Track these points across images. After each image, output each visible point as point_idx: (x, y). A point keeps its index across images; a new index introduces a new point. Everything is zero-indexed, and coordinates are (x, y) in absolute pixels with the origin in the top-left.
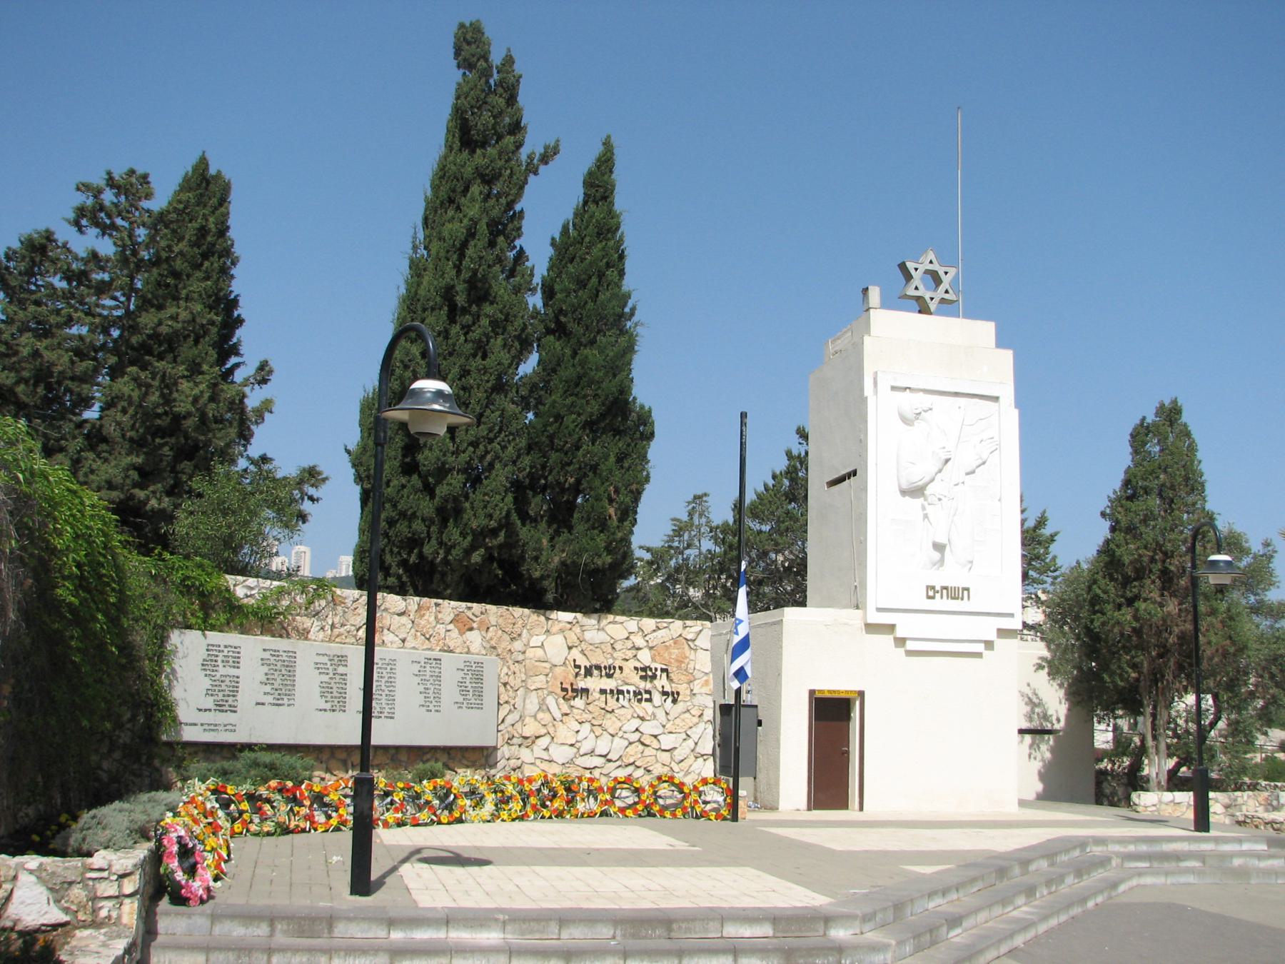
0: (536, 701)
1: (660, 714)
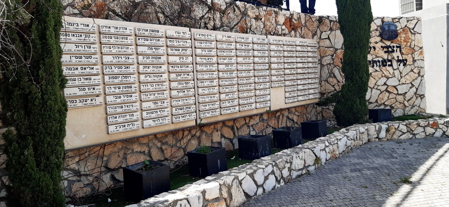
0: (327, 71)
1: (397, 73)
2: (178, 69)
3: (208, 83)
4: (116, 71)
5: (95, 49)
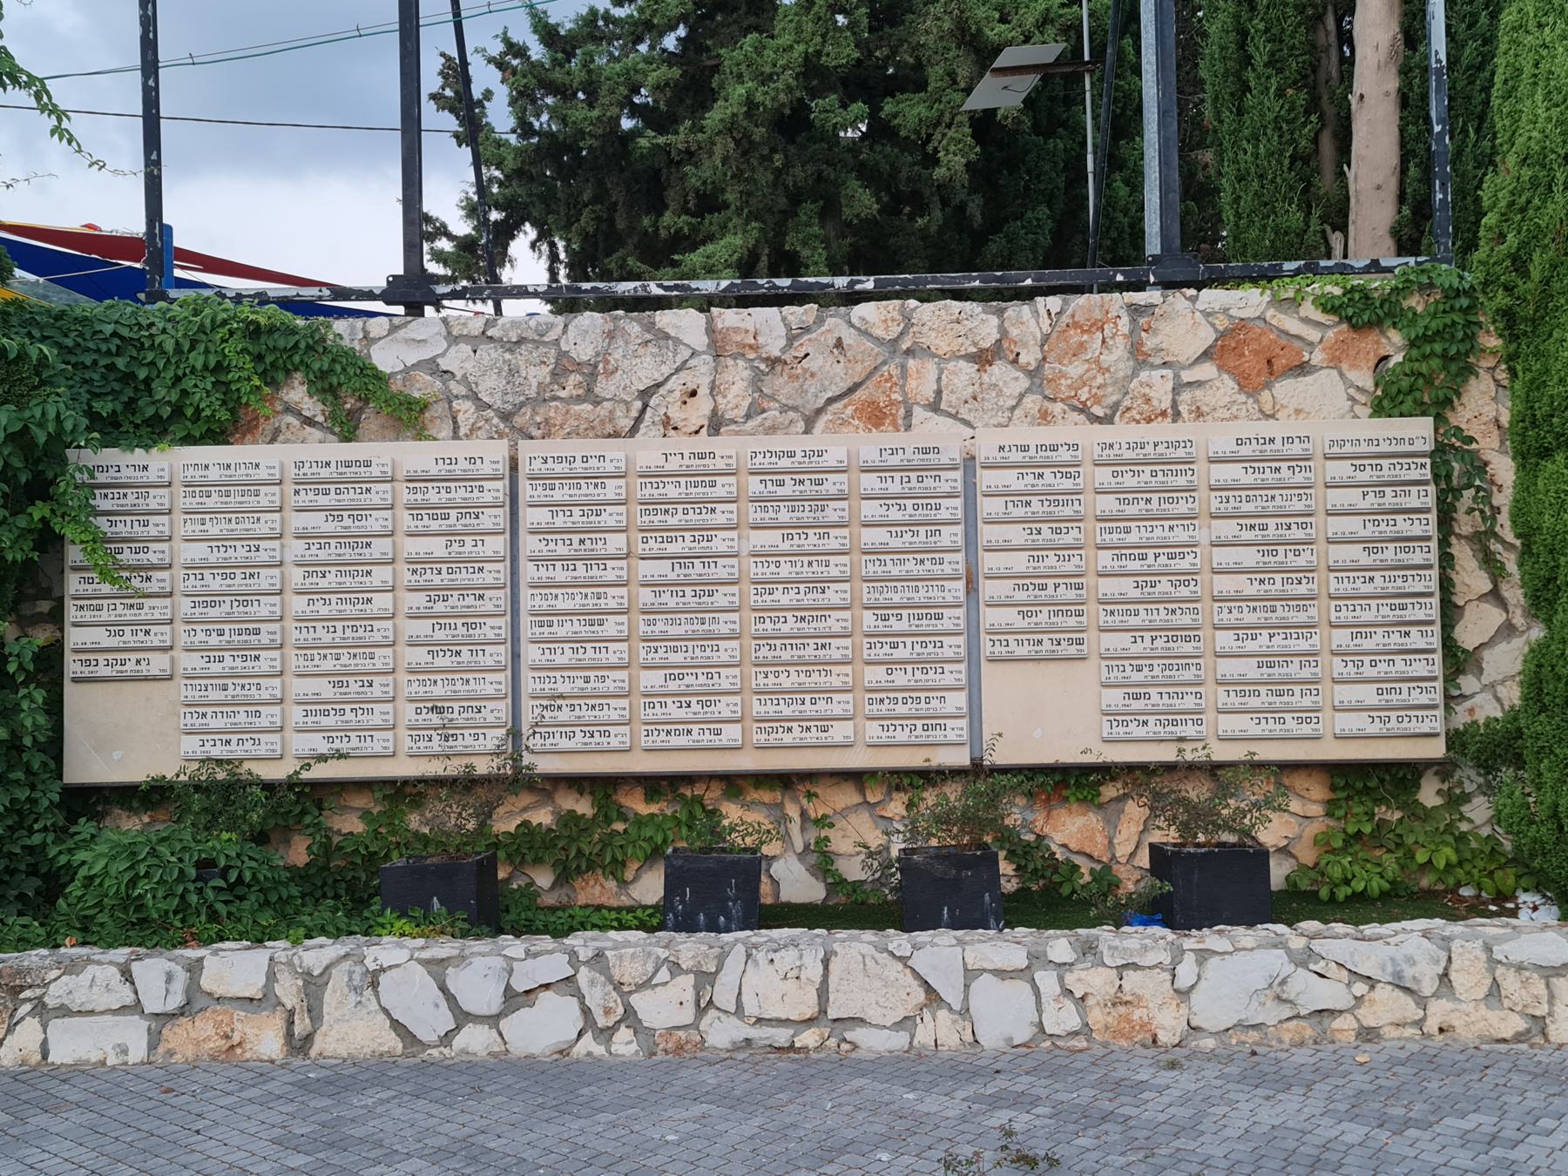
2: (437, 580)
3: (577, 627)
4: (216, 584)
5: (161, 528)
